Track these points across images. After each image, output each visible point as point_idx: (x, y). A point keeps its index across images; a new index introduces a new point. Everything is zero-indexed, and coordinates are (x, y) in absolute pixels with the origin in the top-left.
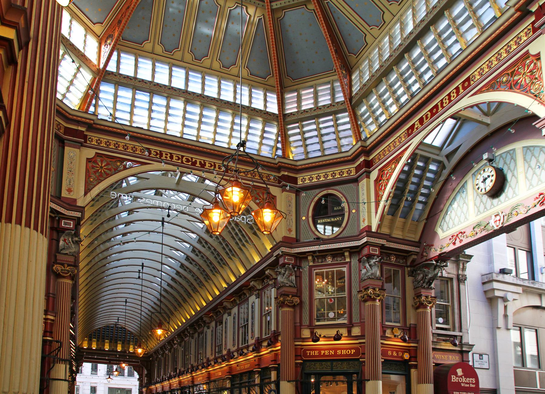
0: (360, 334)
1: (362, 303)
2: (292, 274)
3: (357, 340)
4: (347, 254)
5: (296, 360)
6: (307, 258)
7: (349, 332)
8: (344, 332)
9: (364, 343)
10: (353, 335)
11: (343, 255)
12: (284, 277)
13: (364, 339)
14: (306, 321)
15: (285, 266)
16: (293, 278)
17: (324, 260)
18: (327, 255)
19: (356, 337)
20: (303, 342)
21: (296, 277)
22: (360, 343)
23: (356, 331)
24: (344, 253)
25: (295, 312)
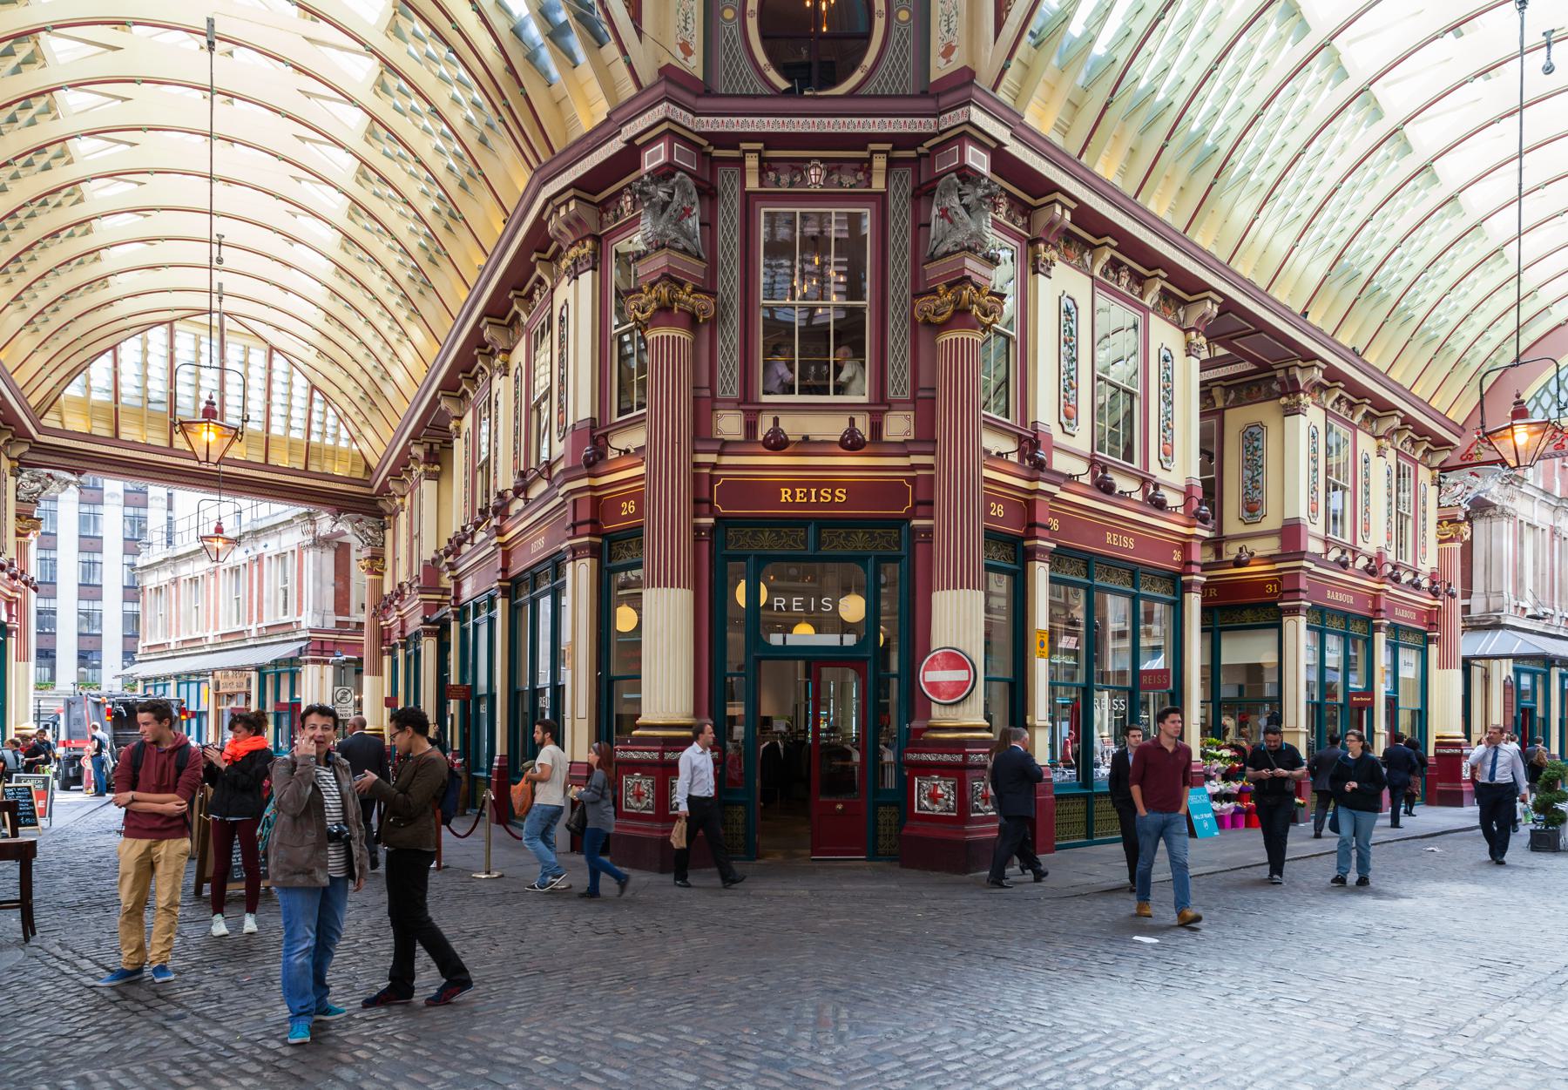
0: (912, 437)
1: (923, 334)
2: (691, 210)
3: (907, 455)
4: (880, 163)
5: (696, 515)
6: (740, 162)
7: (876, 428)
8: (863, 424)
9: (930, 467)
11: (865, 166)
12: (665, 216)
13: (933, 453)
14: (729, 386)
15: (673, 176)
16: (693, 223)
17: (798, 179)
18: (808, 160)
19: (903, 448)
20: (720, 454)
21: (701, 224)
22: (913, 467)
23: (898, 426)
24: (870, 161)
25: (696, 344)
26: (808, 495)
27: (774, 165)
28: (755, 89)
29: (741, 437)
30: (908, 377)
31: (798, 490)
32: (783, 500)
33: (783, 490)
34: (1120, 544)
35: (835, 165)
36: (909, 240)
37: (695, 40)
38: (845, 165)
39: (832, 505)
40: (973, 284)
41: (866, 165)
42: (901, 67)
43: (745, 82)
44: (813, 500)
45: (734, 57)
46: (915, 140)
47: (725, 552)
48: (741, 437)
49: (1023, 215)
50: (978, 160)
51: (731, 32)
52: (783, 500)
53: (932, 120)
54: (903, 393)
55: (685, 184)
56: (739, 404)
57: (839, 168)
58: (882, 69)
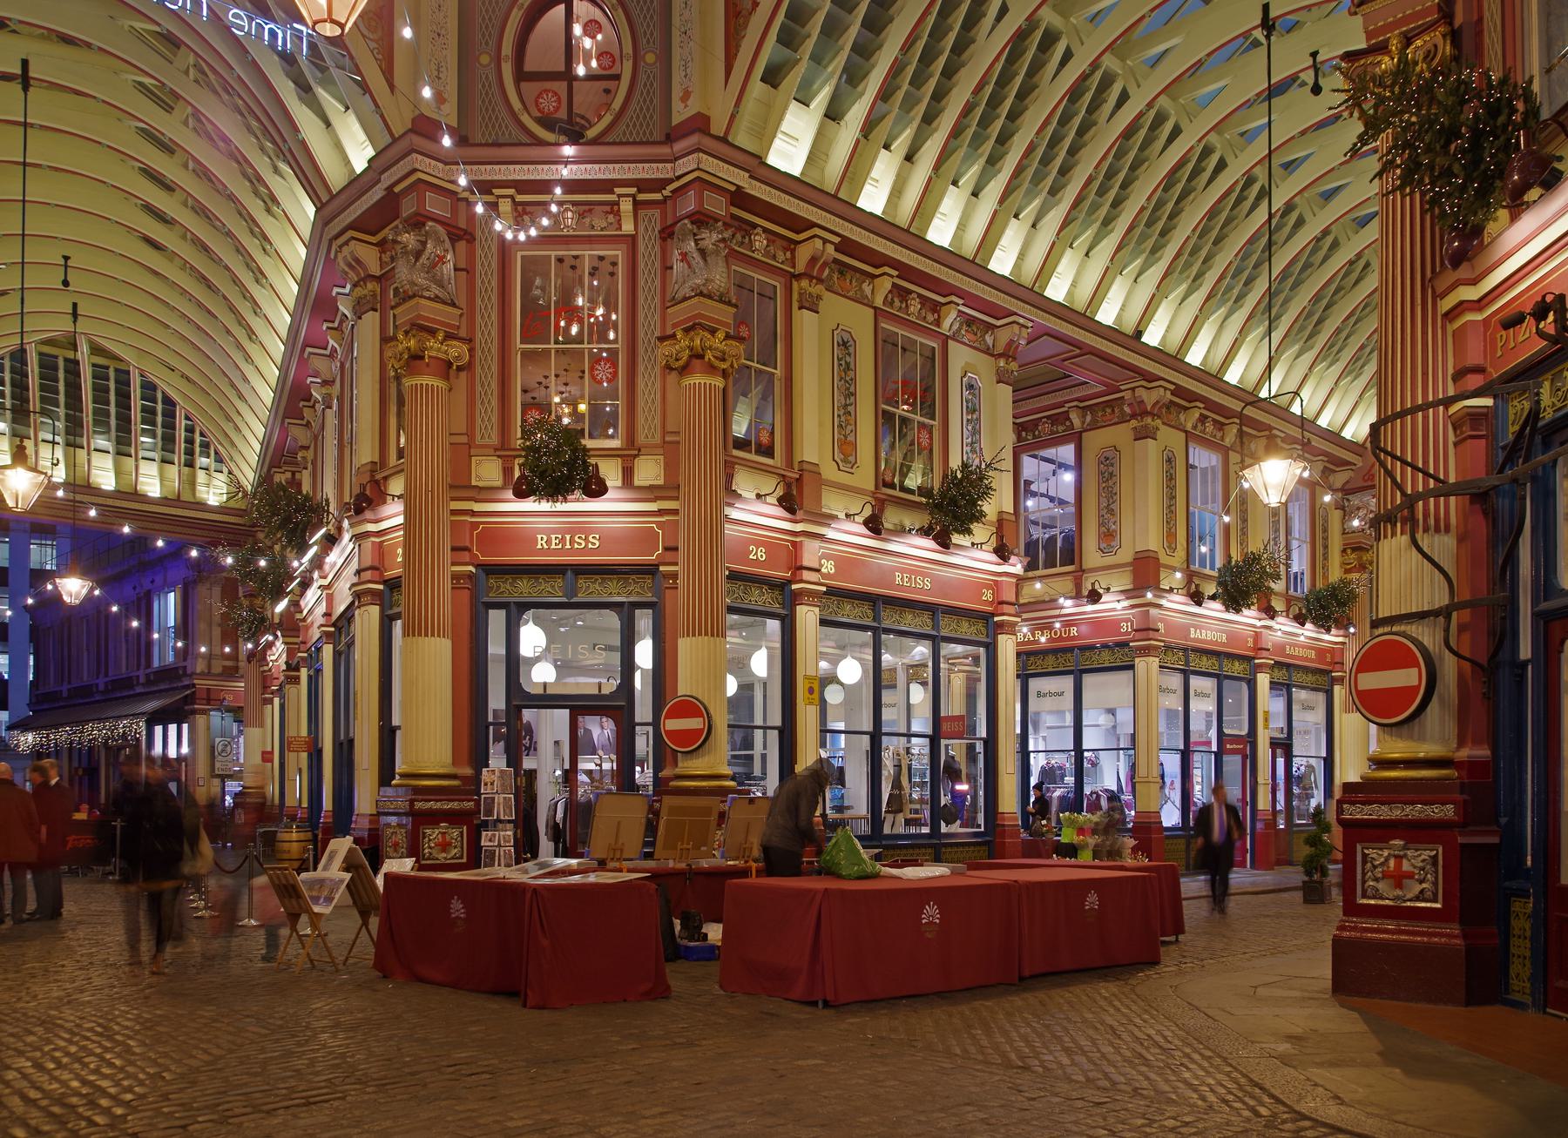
0: (661, 482)
9: (675, 512)
10: (637, 483)
13: (677, 498)
19: (651, 492)
21: (455, 270)
22: (661, 512)
23: (649, 471)
26: (563, 540)
27: (528, 209)
28: (510, 134)
29: (499, 483)
30: (658, 421)
31: (553, 537)
32: (539, 547)
33: (539, 537)
34: (904, 585)
35: (587, 208)
36: (658, 282)
37: (448, 88)
38: (598, 209)
39: (585, 551)
40: (704, 327)
41: (616, 208)
42: (648, 109)
43: (500, 126)
44: (568, 546)
45: (490, 102)
46: (660, 184)
47: (485, 599)
48: (499, 483)
49: (785, 249)
50: (717, 206)
51: (487, 78)
52: (539, 547)
53: (669, 166)
54: (653, 436)
55: (436, 233)
56: (496, 450)
57: (590, 210)
58: (630, 112)
